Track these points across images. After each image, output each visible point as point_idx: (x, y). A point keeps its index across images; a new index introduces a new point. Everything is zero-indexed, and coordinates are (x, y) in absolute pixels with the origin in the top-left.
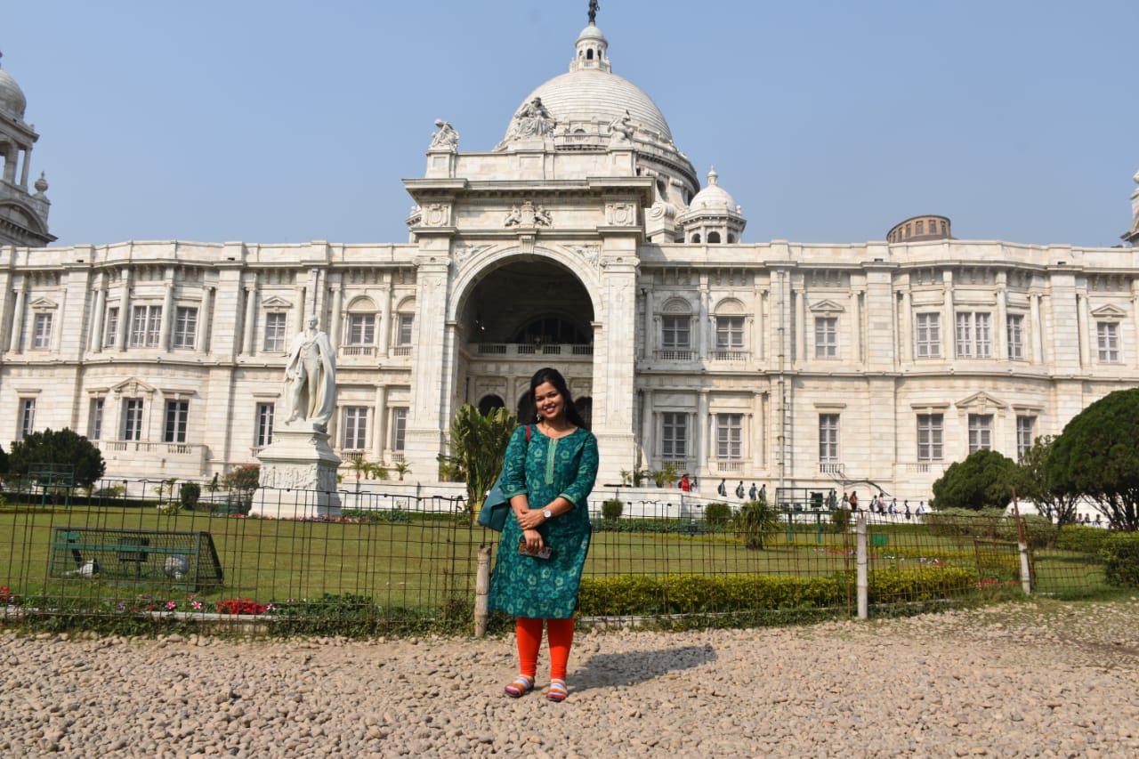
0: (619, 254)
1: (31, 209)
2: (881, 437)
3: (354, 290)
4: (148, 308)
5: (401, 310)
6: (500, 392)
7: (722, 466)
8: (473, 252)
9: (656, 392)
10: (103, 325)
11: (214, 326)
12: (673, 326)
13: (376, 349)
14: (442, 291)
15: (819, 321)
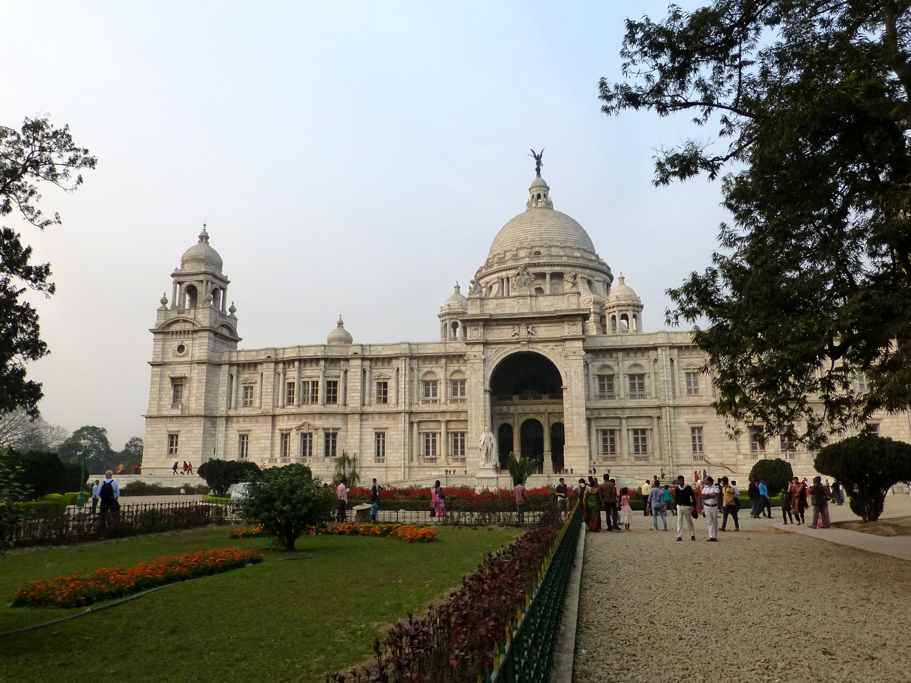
0: (574, 349)
5: (452, 378)
9: (597, 418)
12: (604, 380)
14: (480, 373)
15: (688, 374)
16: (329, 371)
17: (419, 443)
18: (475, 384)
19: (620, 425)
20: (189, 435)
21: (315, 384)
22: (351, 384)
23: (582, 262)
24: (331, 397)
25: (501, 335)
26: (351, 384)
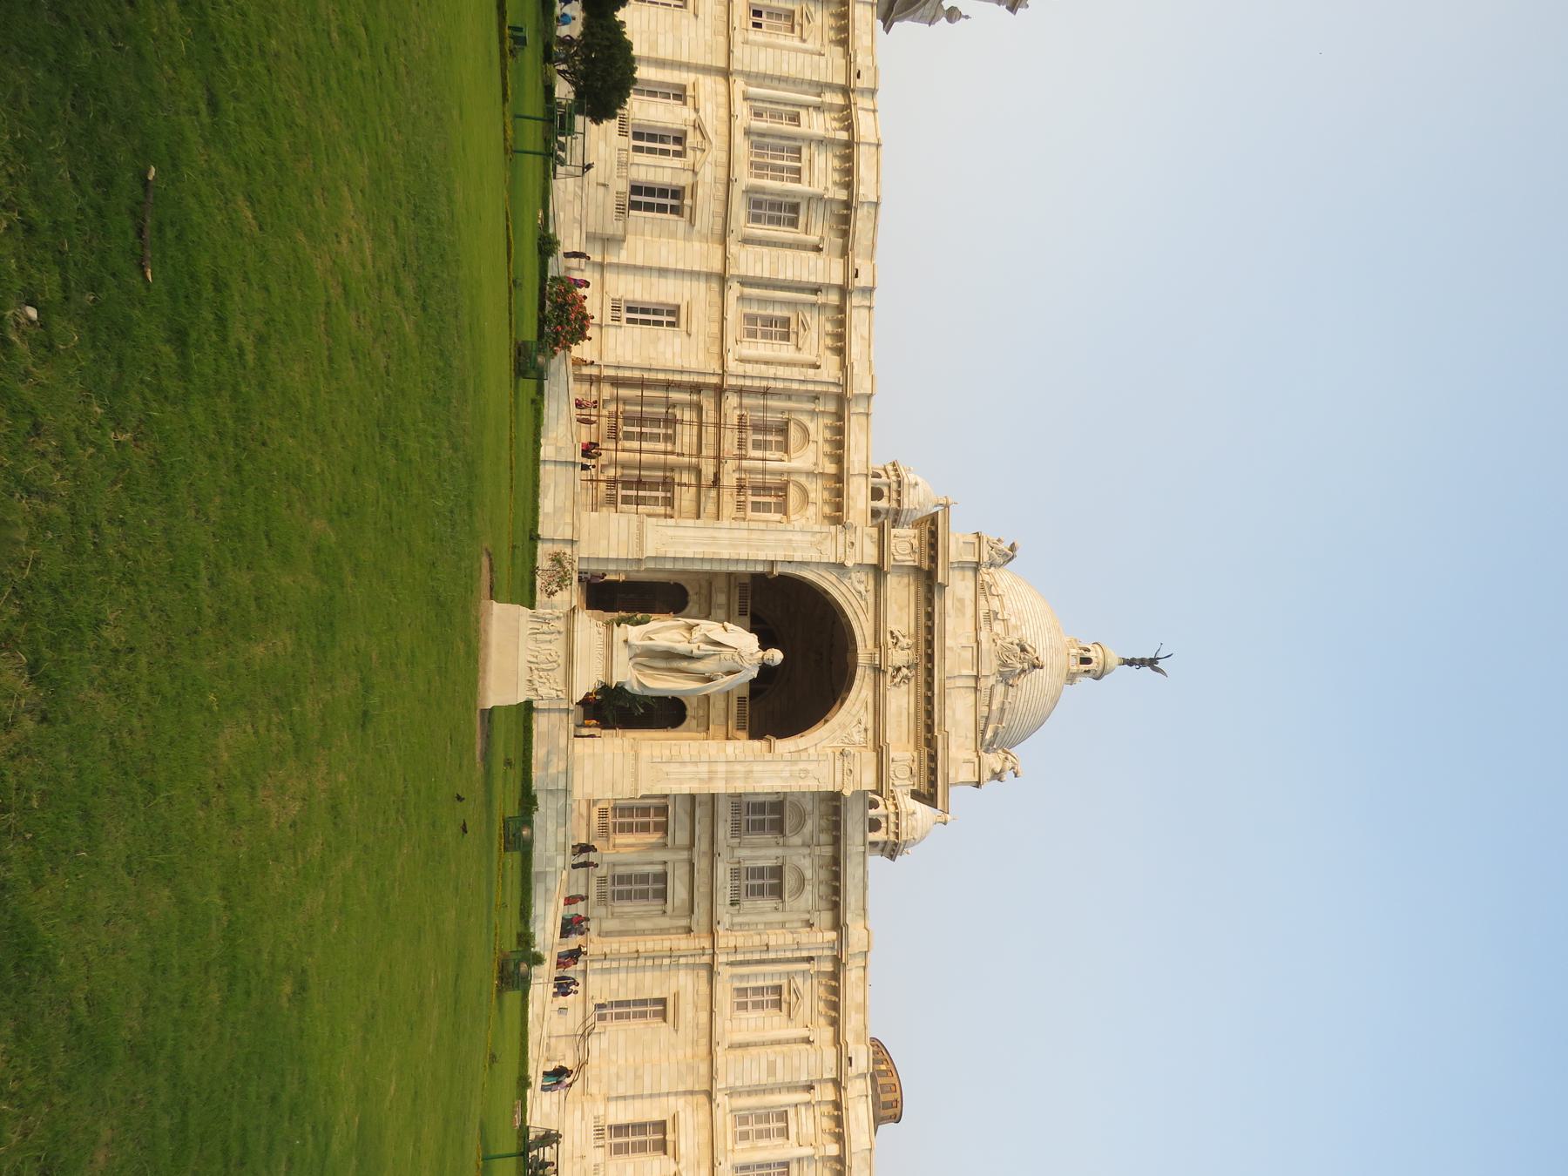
0: (857, 771)
2: (638, 1077)
3: (819, 429)
4: (799, 165)
7: (602, 880)
8: (860, 593)
10: (778, 103)
11: (775, 251)
15: (778, 989)
16: (821, 211)
18: (791, 540)
19: (676, 848)
22: (789, 261)
25: (895, 607)
26: (789, 261)
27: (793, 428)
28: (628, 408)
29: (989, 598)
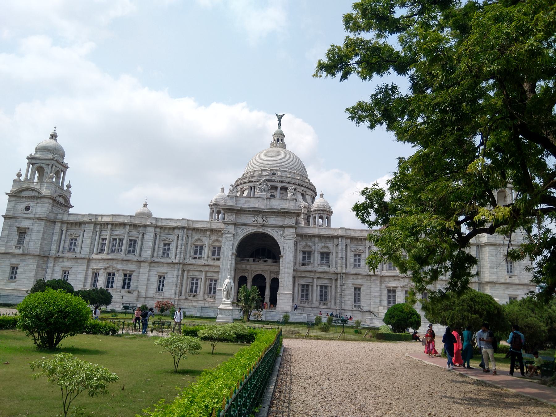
0: (290, 233)
1: (66, 196)
2: (375, 296)
6: (246, 275)
7: (321, 304)
9: (299, 277)
13: (203, 258)
14: (231, 243)
15: (355, 255)
17: (187, 284)
19: (313, 282)
20: (26, 268)
21: (121, 240)
23: (300, 182)
24: (131, 249)
25: (247, 220)
27: (196, 243)
28: (188, 291)
29: (255, 175)
